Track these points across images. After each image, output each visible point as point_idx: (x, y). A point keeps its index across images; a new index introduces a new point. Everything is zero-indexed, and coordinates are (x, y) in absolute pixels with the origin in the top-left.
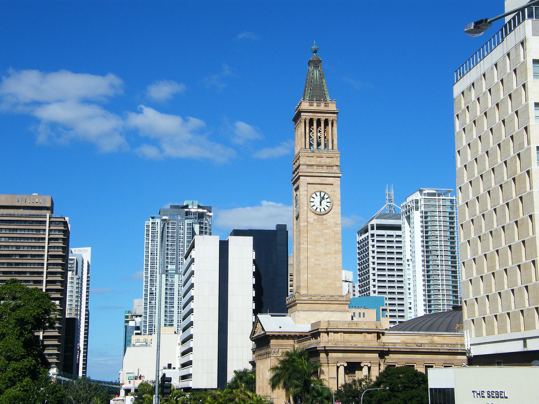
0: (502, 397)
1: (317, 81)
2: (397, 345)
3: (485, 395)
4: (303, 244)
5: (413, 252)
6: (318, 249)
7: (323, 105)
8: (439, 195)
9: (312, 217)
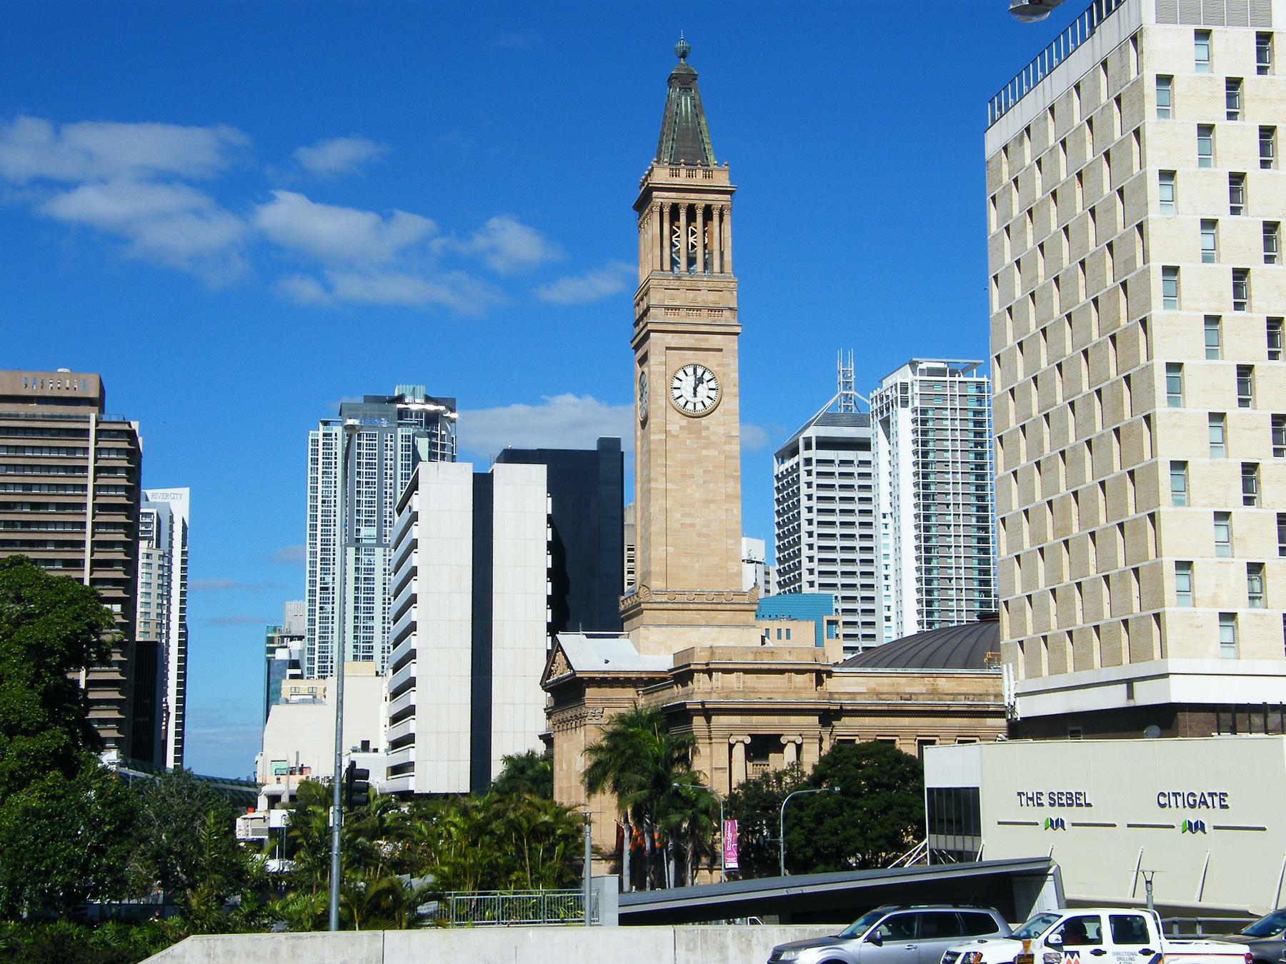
0: (1080, 805)
1: (687, 121)
2: (858, 697)
3: (1045, 800)
4: (656, 480)
5: (895, 497)
6: (689, 491)
7: (700, 173)
8: (952, 374)
9: (676, 423)
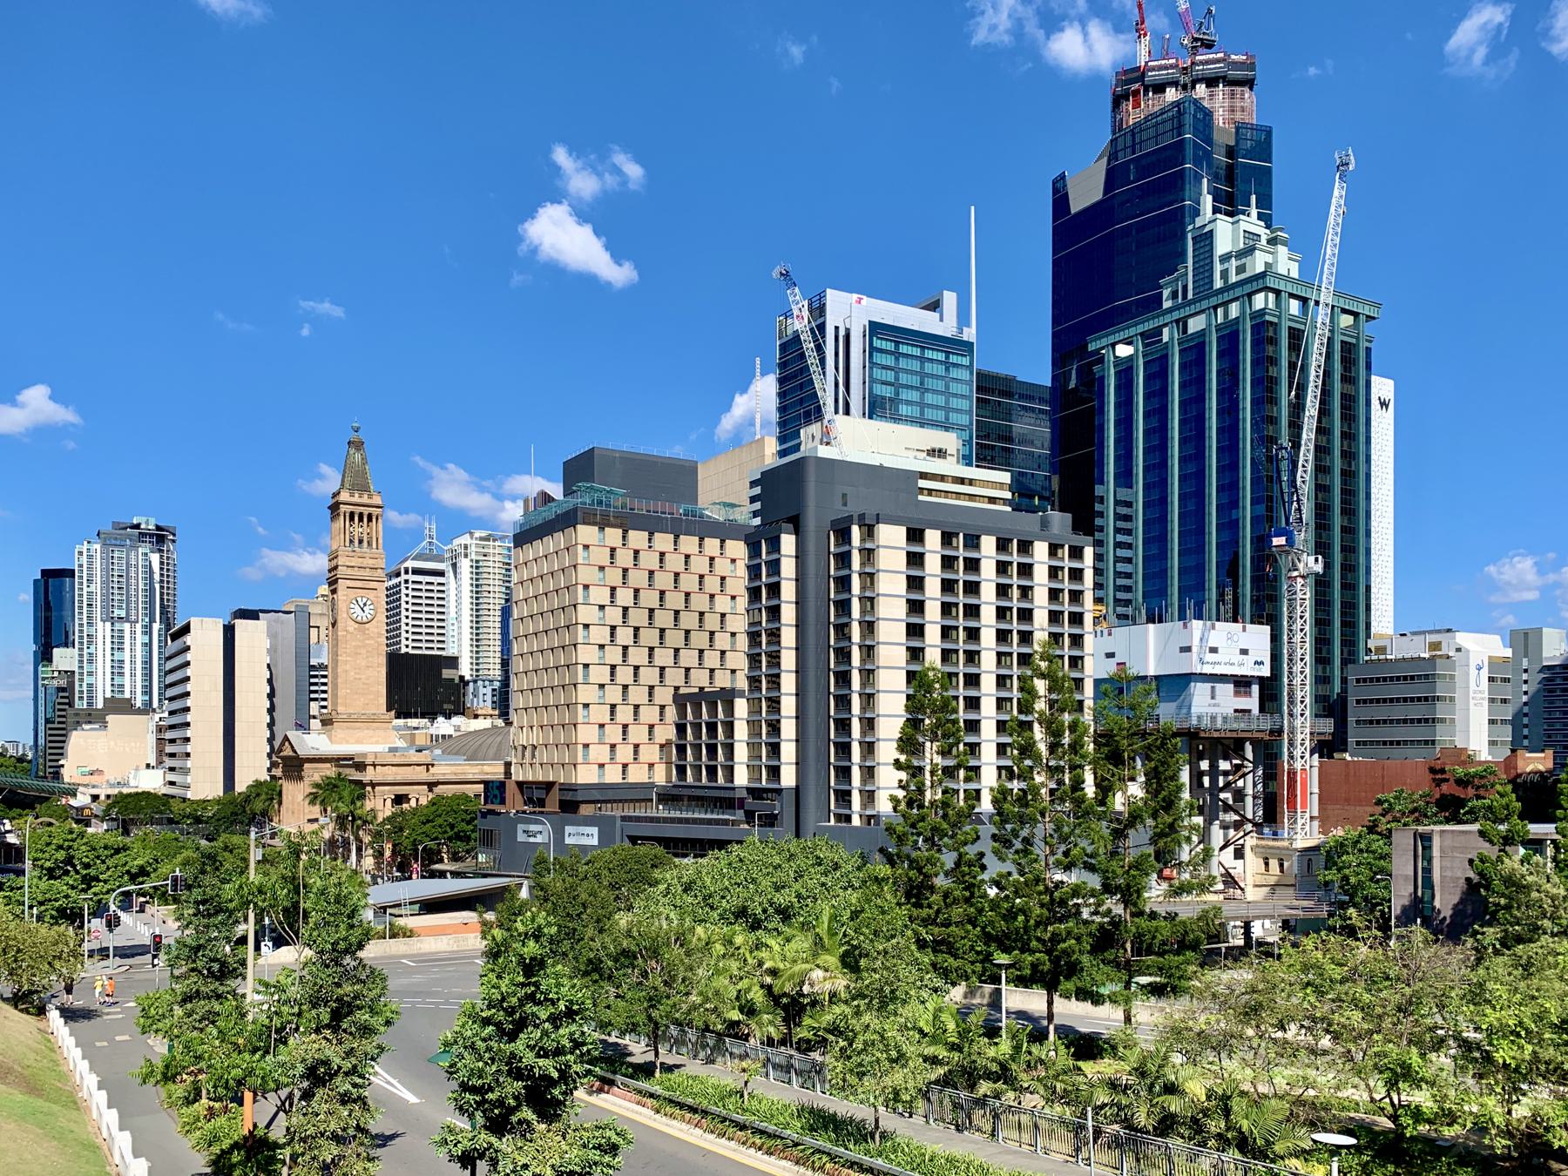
9: (352, 626)
